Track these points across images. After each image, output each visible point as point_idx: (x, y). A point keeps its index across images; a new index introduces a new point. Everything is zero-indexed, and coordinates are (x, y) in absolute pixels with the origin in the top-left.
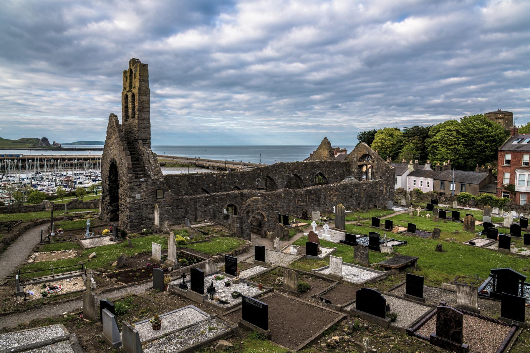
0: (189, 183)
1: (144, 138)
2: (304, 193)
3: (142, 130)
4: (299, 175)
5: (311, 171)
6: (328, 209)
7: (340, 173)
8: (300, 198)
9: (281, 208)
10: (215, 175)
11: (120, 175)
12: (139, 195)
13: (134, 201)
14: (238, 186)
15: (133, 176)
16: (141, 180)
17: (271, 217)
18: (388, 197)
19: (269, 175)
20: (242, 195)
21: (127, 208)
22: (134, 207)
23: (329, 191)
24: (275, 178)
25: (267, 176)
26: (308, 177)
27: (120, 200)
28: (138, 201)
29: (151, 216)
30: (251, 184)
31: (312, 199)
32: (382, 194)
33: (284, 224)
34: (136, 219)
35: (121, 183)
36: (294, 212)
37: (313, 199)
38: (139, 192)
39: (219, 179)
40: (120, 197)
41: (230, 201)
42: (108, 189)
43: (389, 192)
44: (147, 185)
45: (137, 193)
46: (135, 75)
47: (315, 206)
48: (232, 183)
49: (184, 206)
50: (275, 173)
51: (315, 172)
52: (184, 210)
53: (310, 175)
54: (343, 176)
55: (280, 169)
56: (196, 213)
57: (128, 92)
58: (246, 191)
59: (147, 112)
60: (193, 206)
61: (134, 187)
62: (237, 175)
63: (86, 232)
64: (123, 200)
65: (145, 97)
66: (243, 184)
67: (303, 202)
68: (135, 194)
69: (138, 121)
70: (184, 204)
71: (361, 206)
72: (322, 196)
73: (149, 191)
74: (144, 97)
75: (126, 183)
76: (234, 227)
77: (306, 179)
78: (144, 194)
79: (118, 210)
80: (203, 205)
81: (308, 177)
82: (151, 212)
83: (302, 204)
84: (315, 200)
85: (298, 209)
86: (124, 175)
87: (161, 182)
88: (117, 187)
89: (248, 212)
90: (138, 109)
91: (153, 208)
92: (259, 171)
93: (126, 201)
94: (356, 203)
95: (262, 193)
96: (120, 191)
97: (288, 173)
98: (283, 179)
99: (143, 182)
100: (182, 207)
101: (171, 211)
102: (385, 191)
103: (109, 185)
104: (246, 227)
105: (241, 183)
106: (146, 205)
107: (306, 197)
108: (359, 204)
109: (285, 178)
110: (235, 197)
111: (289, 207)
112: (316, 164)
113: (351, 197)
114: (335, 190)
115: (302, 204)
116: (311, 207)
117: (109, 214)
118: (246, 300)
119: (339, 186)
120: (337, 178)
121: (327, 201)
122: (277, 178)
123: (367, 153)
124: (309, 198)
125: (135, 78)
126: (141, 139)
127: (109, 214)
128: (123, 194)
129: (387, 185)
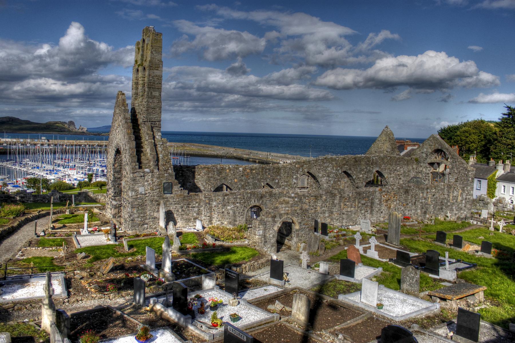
0: (209, 177)
1: (153, 120)
2: (352, 196)
4: (349, 172)
5: (366, 168)
6: (383, 217)
7: (404, 172)
8: (348, 202)
9: (321, 213)
11: (124, 163)
13: (137, 195)
14: (271, 184)
16: (147, 170)
17: (304, 225)
18: (463, 205)
19: (311, 172)
20: (271, 195)
21: (129, 204)
23: (386, 195)
24: (318, 176)
25: (308, 172)
26: (361, 176)
27: (123, 193)
28: (141, 196)
29: (156, 214)
30: (286, 182)
31: (363, 204)
32: (456, 201)
33: (322, 234)
34: (138, 217)
35: (124, 173)
36: (337, 219)
37: (364, 204)
38: (143, 186)
40: (123, 189)
41: (255, 201)
42: (112, 179)
43: (466, 199)
44: (153, 176)
45: (140, 186)
46: (147, 46)
47: (367, 213)
48: (263, 179)
49: (197, 205)
50: (319, 169)
51: (371, 169)
52: (196, 209)
53: (365, 174)
54: (408, 176)
55: (326, 165)
56: (211, 214)
57: (139, 65)
58: (276, 191)
59: (158, 89)
60: (208, 205)
61: (138, 178)
63: (83, 228)
64: (125, 193)
65: (156, 71)
66: (277, 181)
67: (352, 207)
68: (139, 187)
69: (147, 100)
70: (197, 203)
71: (427, 216)
72: (377, 201)
74: (155, 71)
75: (129, 173)
76: (255, 235)
77: (358, 178)
78: (149, 187)
79: (120, 206)
81: (361, 176)
82: (156, 210)
83: (349, 209)
84: (367, 206)
85: (344, 216)
86: (128, 164)
87: (169, 173)
88: (120, 179)
89: (274, 217)
90: (148, 85)
91: (159, 205)
93: (128, 195)
94: (421, 211)
95: (297, 194)
96: (123, 183)
97: (336, 170)
98: (328, 176)
99: (148, 173)
100: (194, 206)
101: (180, 210)
102: (460, 198)
103: (114, 175)
104: (271, 236)
105: (273, 179)
107: (355, 201)
108: (425, 213)
109: (332, 175)
110: (262, 197)
111: (332, 213)
112: (373, 159)
113: (415, 203)
114: (394, 194)
115: (349, 209)
116: (362, 214)
117: (113, 209)
118: (229, 329)
119: (399, 189)
120: (400, 179)
121: (383, 208)
122: (320, 175)
123: (440, 148)
124: (359, 202)
125: (147, 49)
126: (149, 121)
127: (113, 209)
128: (126, 186)
129: (463, 190)
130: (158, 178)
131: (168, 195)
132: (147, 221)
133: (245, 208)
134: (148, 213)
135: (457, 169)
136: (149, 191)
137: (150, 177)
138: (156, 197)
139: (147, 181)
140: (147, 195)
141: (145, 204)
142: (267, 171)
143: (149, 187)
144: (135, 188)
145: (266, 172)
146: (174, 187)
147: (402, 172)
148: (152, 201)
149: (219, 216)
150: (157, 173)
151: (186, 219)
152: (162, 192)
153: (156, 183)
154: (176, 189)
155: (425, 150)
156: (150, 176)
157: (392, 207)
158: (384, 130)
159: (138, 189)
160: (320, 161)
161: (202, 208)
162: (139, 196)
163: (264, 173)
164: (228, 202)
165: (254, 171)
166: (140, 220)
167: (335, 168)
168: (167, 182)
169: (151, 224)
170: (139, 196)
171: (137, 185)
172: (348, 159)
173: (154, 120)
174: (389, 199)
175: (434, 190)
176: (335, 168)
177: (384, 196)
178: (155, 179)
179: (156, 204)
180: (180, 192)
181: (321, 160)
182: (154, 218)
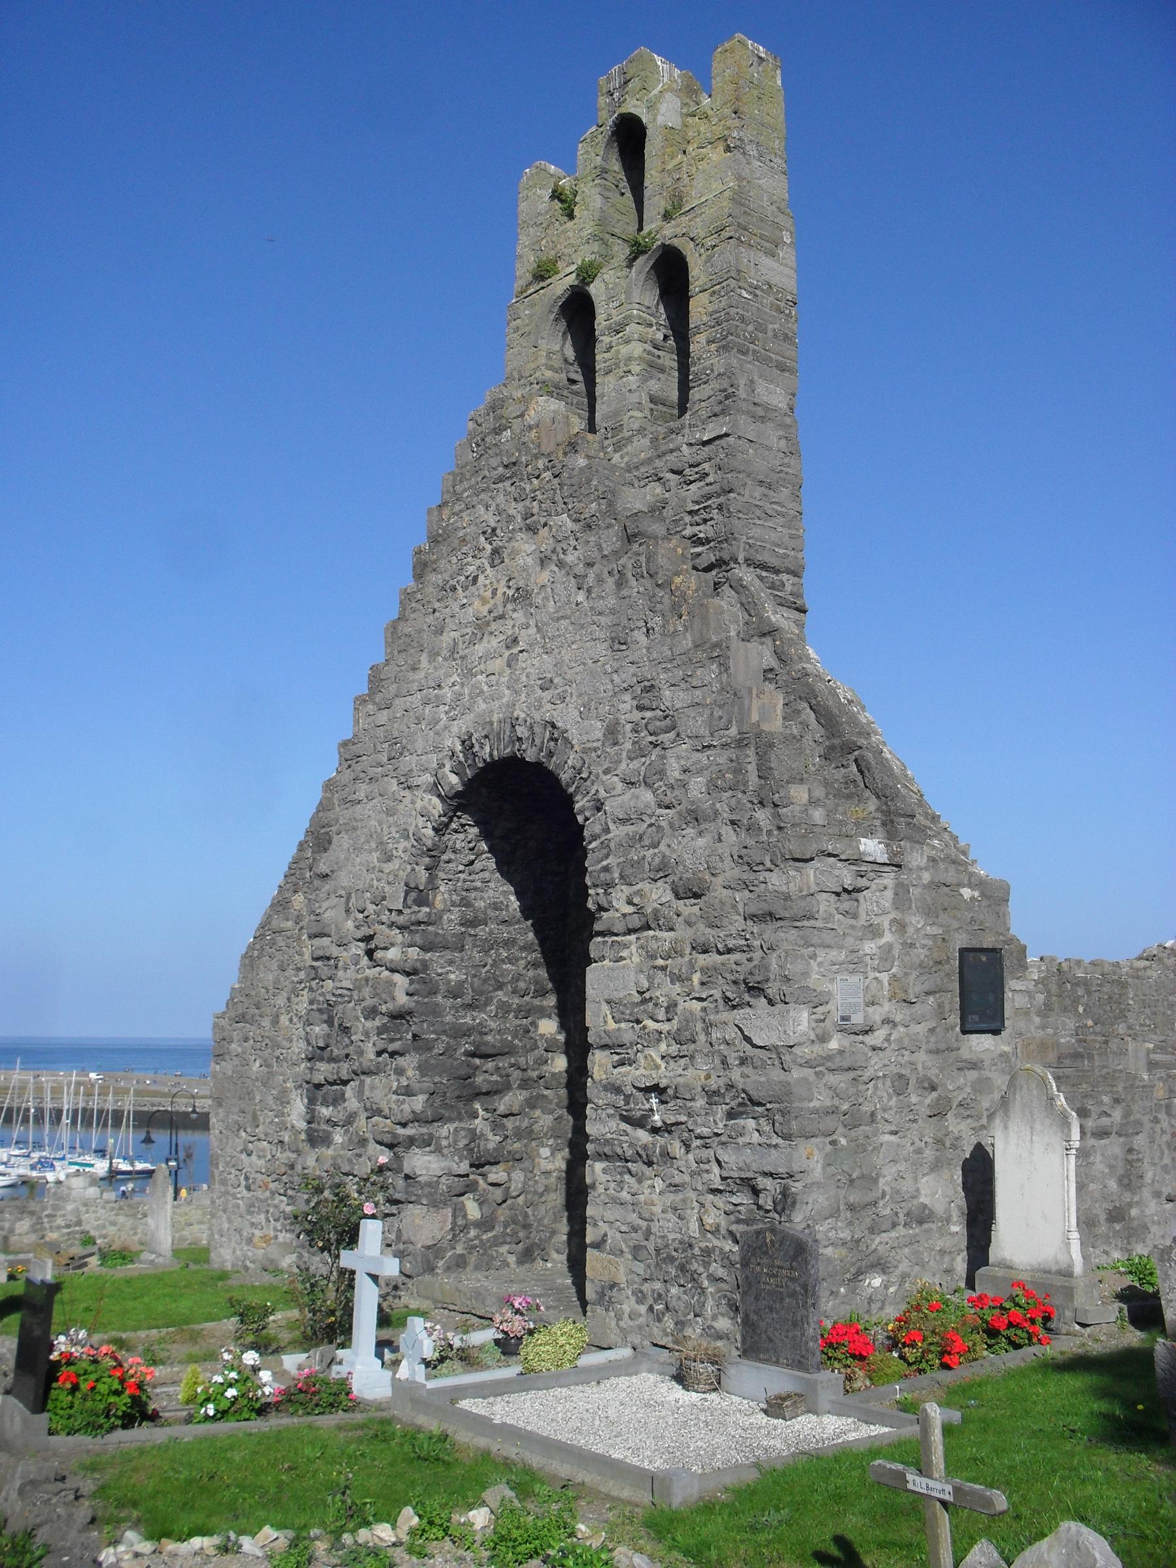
3: (759, 491)
13: (823, 1039)
15: (813, 802)
22: (821, 1100)
34: (835, 1213)
38: (855, 964)
62: (1085, 983)
65: (767, 261)
100: (1105, 1121)
106: (900, 1084)
126: (749, 562)
130: (931, 912)
134: (888, 1174)
138: (922, 1057)
139: (874, 931)
141: (866, 1108)
143: (885, 977)
144: (811, 983)
148: (900, 1084)
152: (955, 1019)
153: (920, 953)
156: (889, 894)
159: (827, 986)
161: (1140, 1141)
162: (834, 1045)
163: (1068, 1002)
166: (845, 1234)
169: (904, 1267)
170: (834, 1045)
171: (821, 954)
173: (774, 562)
178: (916, 921)
179: (924, 1111)
180: (1037, 1020)
182: (921, 1222)
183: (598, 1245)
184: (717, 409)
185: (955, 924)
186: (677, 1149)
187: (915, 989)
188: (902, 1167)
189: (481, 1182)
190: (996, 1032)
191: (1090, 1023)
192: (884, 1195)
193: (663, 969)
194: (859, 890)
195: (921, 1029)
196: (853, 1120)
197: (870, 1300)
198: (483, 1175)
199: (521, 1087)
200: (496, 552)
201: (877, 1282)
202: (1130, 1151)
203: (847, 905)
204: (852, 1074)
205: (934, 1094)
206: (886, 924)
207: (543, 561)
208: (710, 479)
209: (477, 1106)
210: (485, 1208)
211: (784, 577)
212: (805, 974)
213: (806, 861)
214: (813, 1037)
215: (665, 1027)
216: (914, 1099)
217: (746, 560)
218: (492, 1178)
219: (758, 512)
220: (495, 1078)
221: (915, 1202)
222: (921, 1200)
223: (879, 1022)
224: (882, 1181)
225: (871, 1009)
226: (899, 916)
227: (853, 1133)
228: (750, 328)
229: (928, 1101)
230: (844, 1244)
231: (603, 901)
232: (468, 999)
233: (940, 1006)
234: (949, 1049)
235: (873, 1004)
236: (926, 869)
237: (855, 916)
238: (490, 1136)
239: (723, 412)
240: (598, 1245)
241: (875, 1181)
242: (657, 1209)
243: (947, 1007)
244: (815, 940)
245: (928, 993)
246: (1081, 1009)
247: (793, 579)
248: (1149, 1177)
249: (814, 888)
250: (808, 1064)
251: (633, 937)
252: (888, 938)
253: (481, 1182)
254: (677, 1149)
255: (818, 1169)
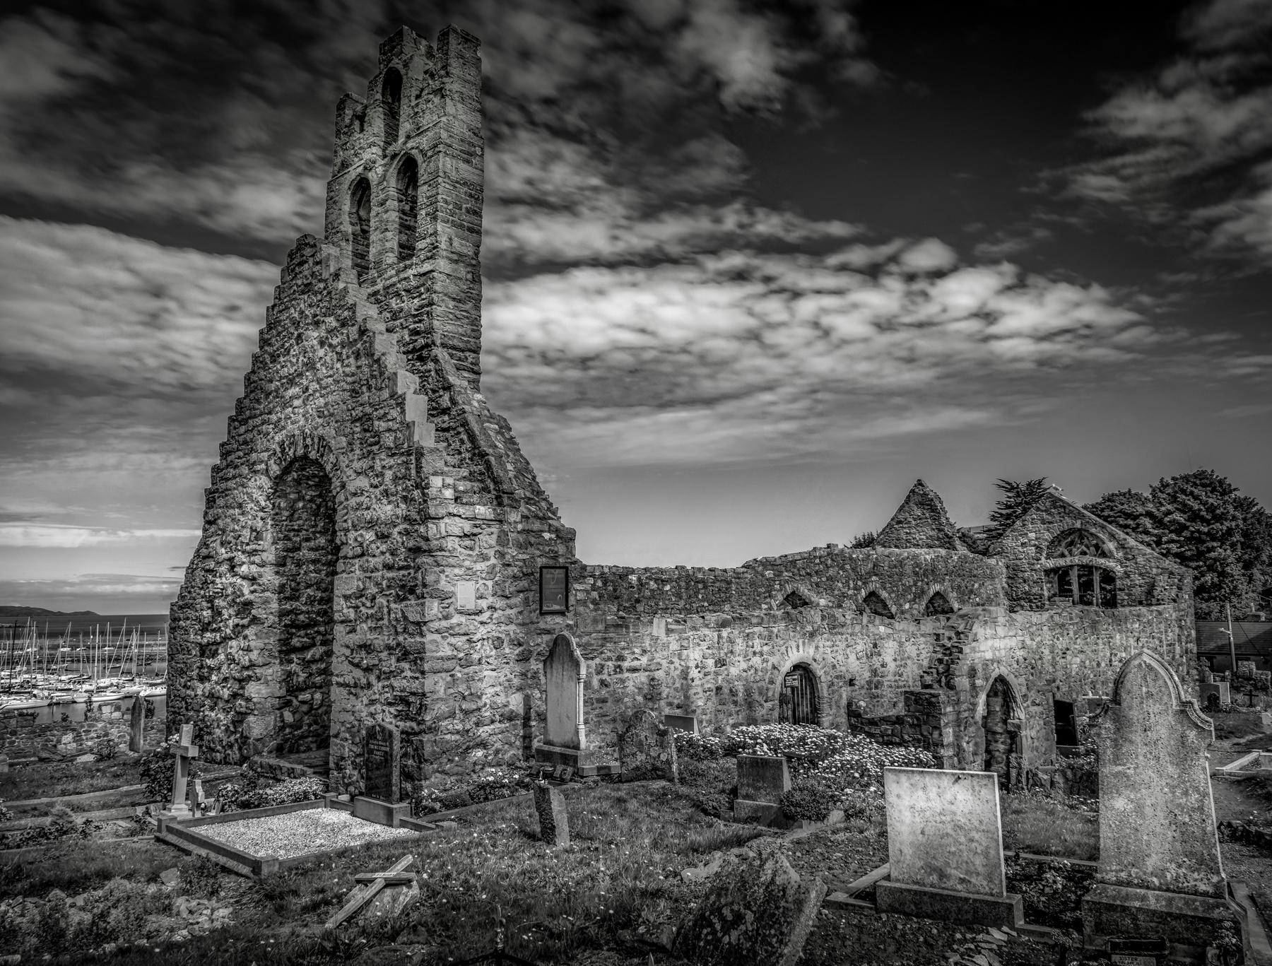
1: (456, 342)
5: (915, 585)
10: (633, 578)
12: (471, 586)
15: (445, 486)
17: (1034, 704)
22: (448, 652)
28: (463, 619)
34: (452, 715)
38: (470, 574)
39: (648, 593)
44: (502, 540)
50: (817, 585)
51: (925, 586)
55: (831, 572)
56: (687, 697)
62: (703, 581)
73: (510, 571)
78: (490, 583)
80: (710, 662)
92: (769, 573)
97: (855, 589)
100: (636, 663)
113: (1111, 661)
114: (1075, 633)
126: (444, 345)
130: (520, 546)
131: (559, 619)
132: (483, 732)
133: (776, 672)
135: (1140, 574)
136: (491, 599)
137: (493, 540)
140: (485, 617)
141: (476, 656)
142: (700, 586)
143: (490, 583)
145: (696, 593)
146: (577, 586)
147: (984, 596)
149: (709, 703)
150: (520, 527)
151: (614, 720)
154: (580, 596)
155: (1032, 535)
156: (495, 536)
157: (1073, 673)
158: (913, 491)
160: (817, 561)
162: (454, 621)
164: (732, 652)
165: (667, 588)
166: (460, 727)
167: (851, 582)
168: (551, 562)
170: (454, 621)
171: (448, 570)
172: (877, 559)
173: (461, 345)
174: (1068, 649)
175: (1137, 626)
176: (851, 582)
177: (1058, 639)
178: (512, 551)
180: (592, 606)
181: (820, 557)
183: (336, 736)
184: (429, 254)
185: (538, 553)
186: (373, 679)
187: (510, 588)
188: (498, 689)
189: (294, 700)
190: (562, 613)
191: (706, 604)
192: (485, 705)
193: (370, 578)
194: (475, 535)
195: (513, 612)
196: (466, 662)
197: (475, 764)
198: (296, 697)
199: (321, 644)
200: (299, 336)
201: (480, 753)
202: (653, 679)
203: (467, 542)
204: (467, 637)
205: (521, 648)
206: (492, 553)
207: (322, 343)
208: (424, 296)
209: (293, 656)
210: (296, 716)
211: (467, 354)
212: (437, 582)
213: (439, 519)
214: (440, 616)
215: (370, 612)
216: (507, 651)
217: (442, 344)
218: (301, 697)
219: (451, 316)
220: (305, 639)
221: (507, 709)
222: (511, 707)
223: (485, 608)
224: (484, 697)
225: (480, 601)
226: (501, 549)
227: (466, 670)
228: (451, 207)
229: (517, 652)
230: (458, 732)
231: (344, 539)
232: (288, 594)
233: (527, 599)
234: (532, 623)
235: (481, 598)
236: (521, 522)
237: (471, 549)
238: (301, 673)
239: (431, 258)
240: (336, 736)
241: (480, 698)
242: (364, 714)
243: (531, 599)
244: (444, 563)
245: (519, 592)
246: (700, 596)
247: (473, 355)
248: (664, 695)
249: (444, 534)
250: (437, 631)
251: (357, 561)
252: (493, 561)
253: (294, 700)
254: (373, 679)
255: (442, 690)
